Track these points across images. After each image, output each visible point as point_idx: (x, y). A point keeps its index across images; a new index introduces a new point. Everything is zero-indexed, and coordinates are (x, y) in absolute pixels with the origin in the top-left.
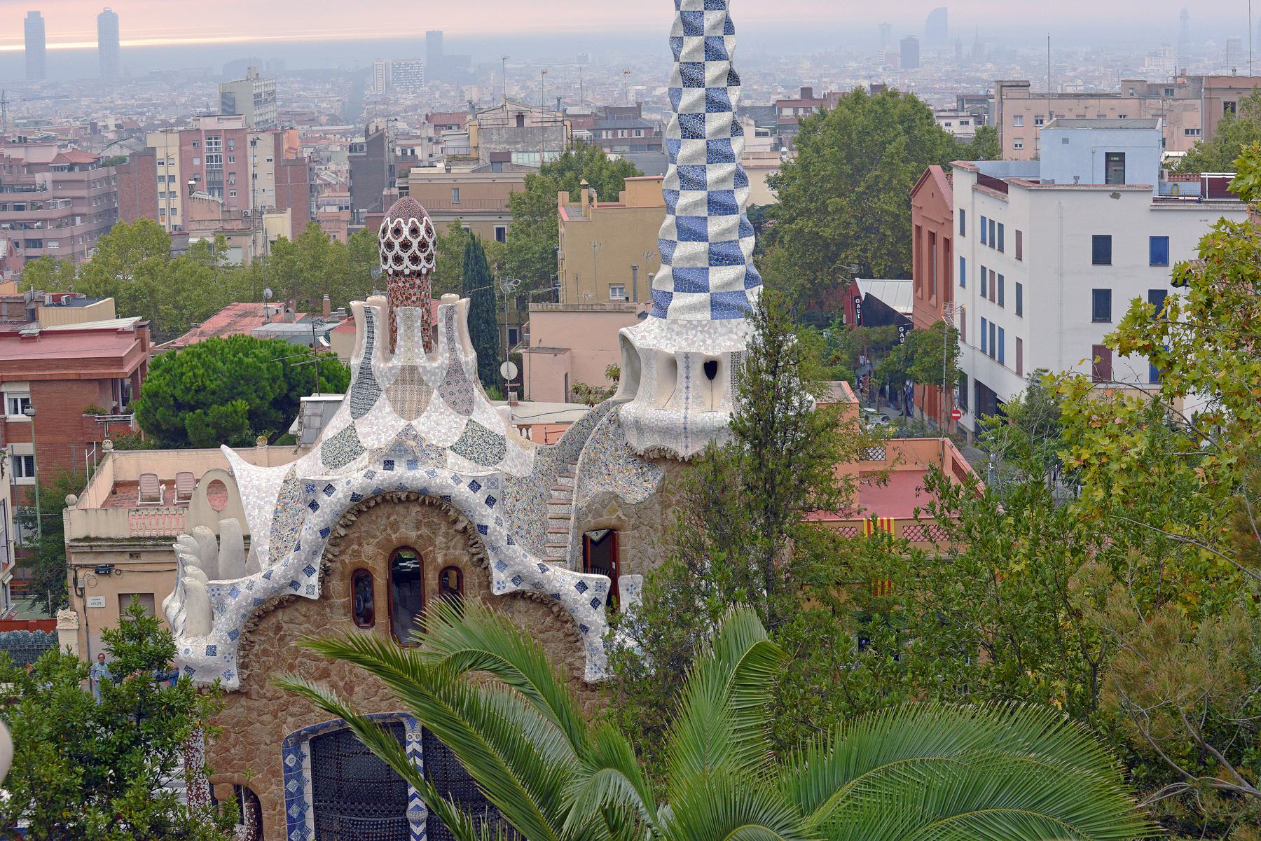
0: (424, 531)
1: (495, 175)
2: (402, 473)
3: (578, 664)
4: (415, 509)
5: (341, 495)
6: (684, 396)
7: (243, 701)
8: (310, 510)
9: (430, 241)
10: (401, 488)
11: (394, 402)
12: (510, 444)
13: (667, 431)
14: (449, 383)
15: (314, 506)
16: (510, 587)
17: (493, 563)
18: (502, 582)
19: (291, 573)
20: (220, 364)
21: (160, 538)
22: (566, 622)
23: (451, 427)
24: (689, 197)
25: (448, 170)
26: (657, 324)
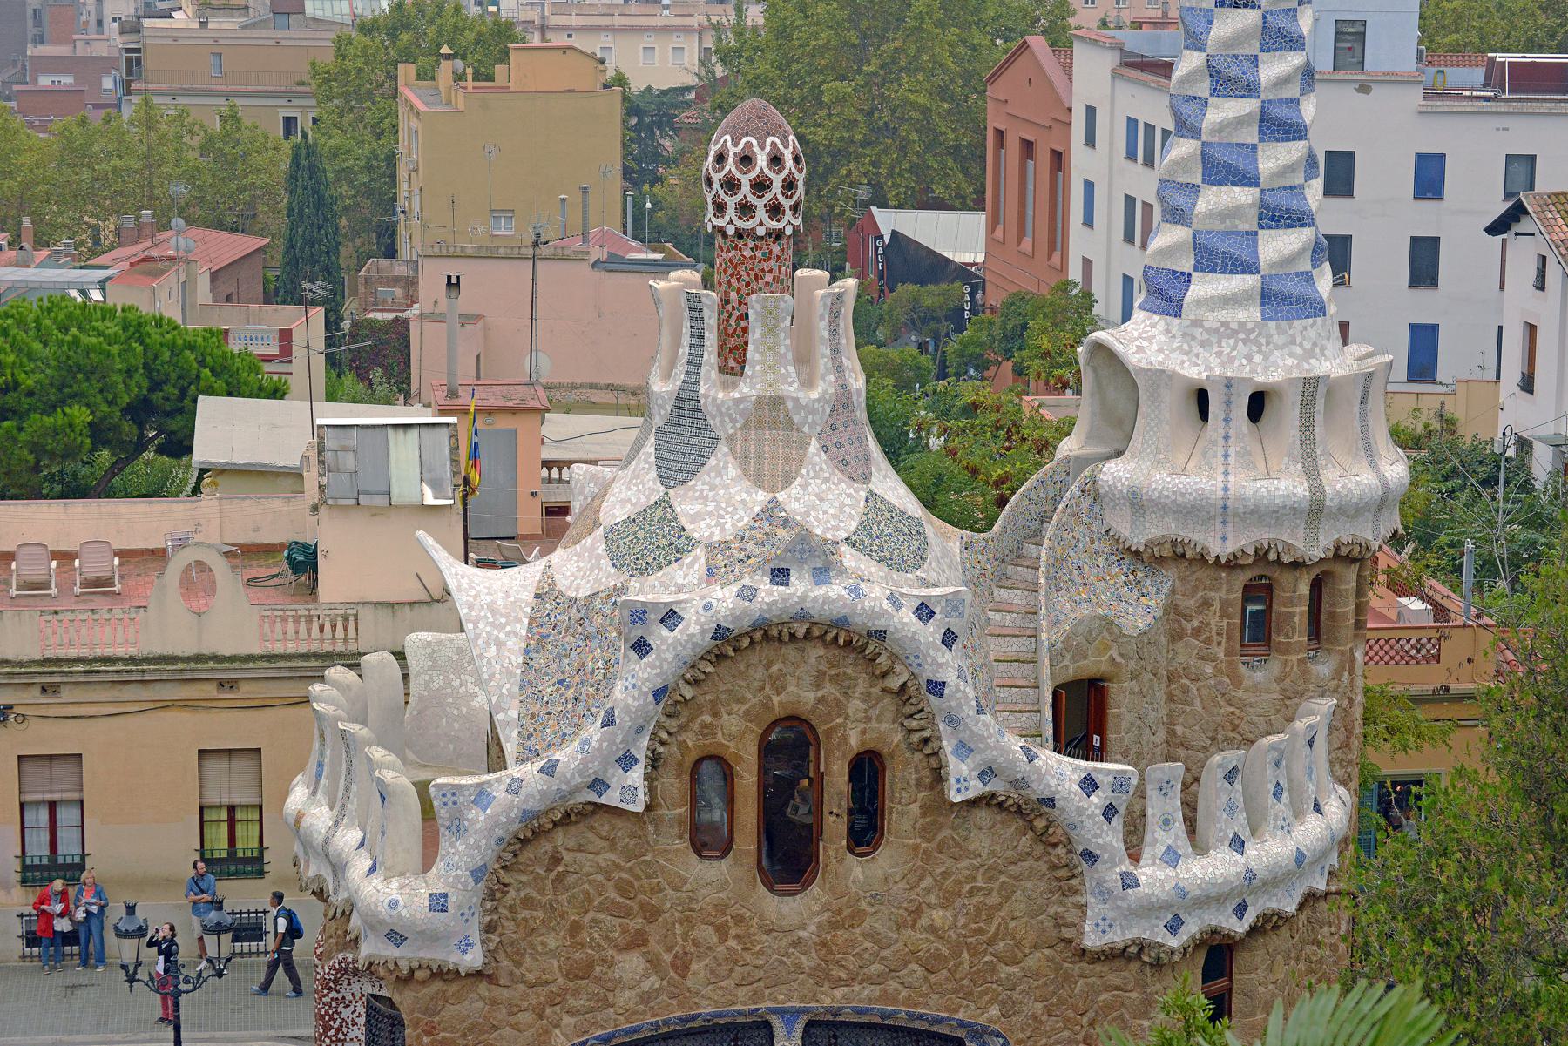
0: (829, 690)
1: (279, 34)
2: (801, 588)
3: (1072, 916)
4: (815, 652)
5: (694, 629)
6: (1221, 452)
7: (483, 988)
8: (632, 653)
9: (800, 178)
10: (802, 616)
11: (743, 460)
12: (929, 531)
13: (1192, 510)
14: (833, 428)
15: (641, 647)
16: (976, 788)
17: (948, 746)
18: (963, 781)
19: (594, 767)
20: (37, 346)
21: (96, 660)
22: (1055, 845)
23: (842, 505)
24: (1223, 111)
25: (204, 24)
26: (1161, 326)
